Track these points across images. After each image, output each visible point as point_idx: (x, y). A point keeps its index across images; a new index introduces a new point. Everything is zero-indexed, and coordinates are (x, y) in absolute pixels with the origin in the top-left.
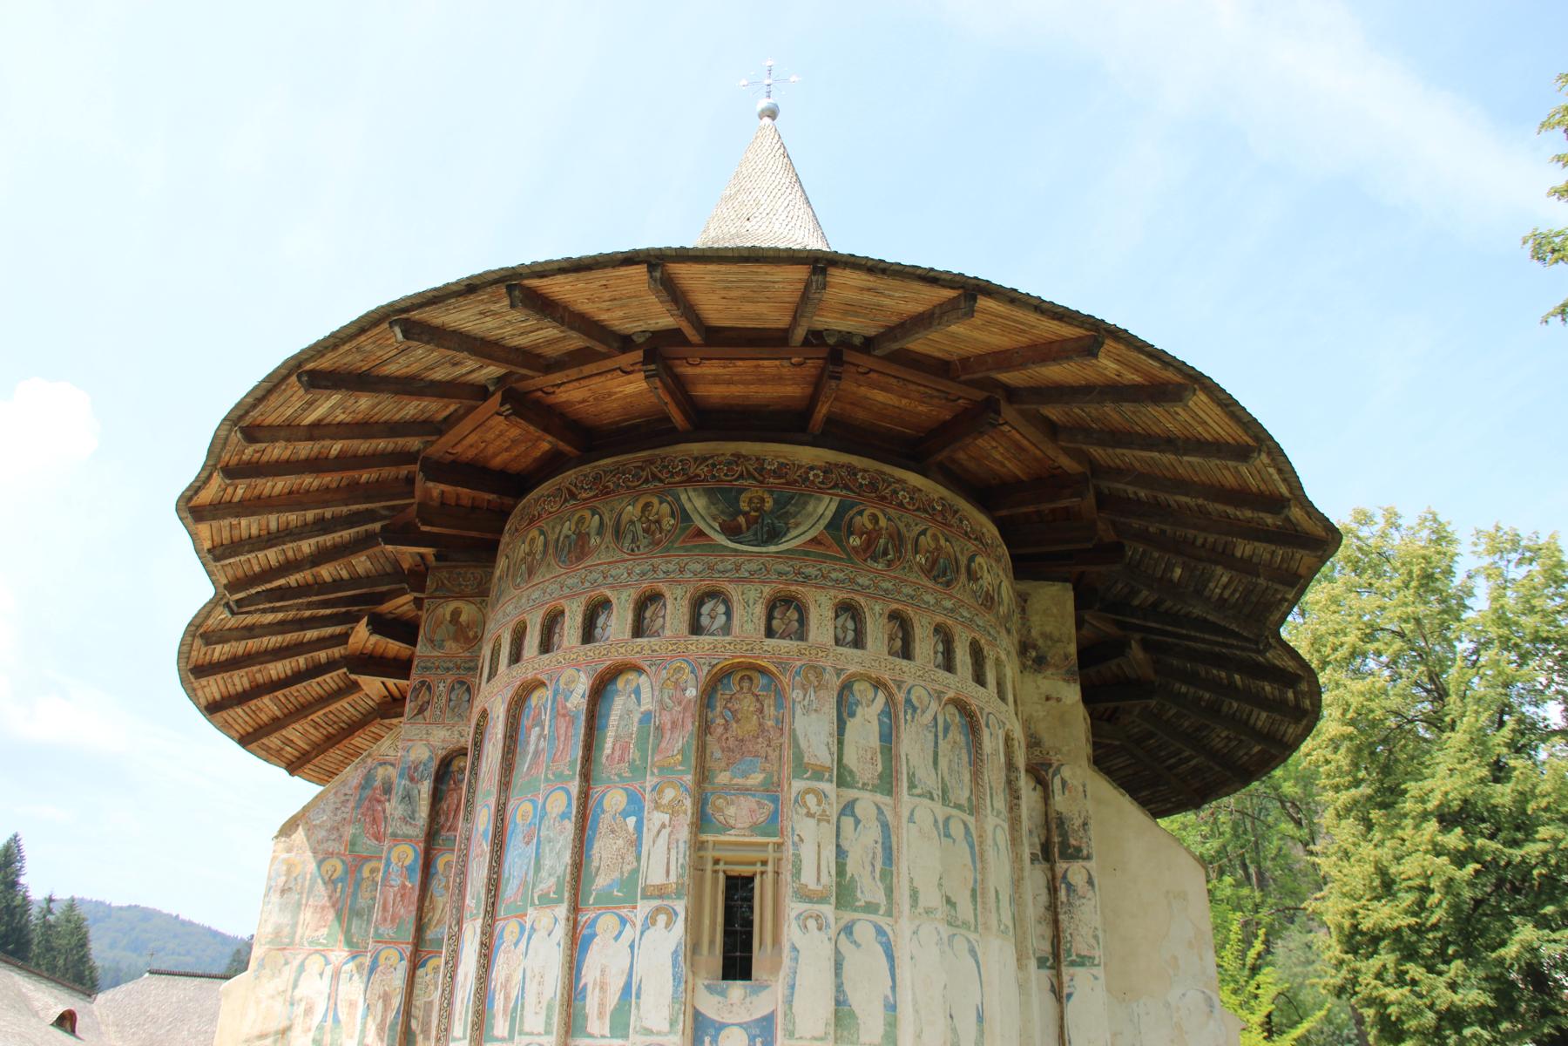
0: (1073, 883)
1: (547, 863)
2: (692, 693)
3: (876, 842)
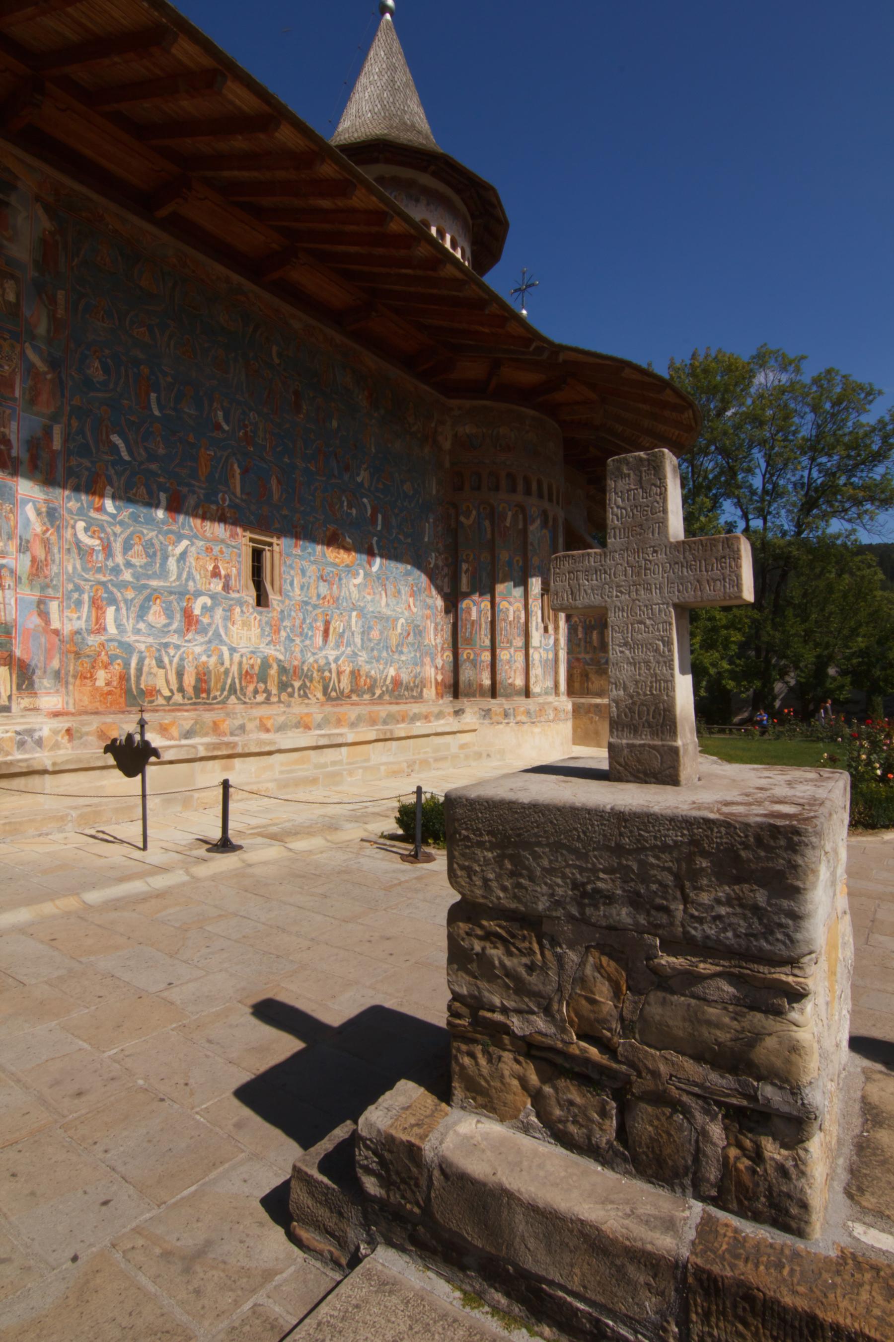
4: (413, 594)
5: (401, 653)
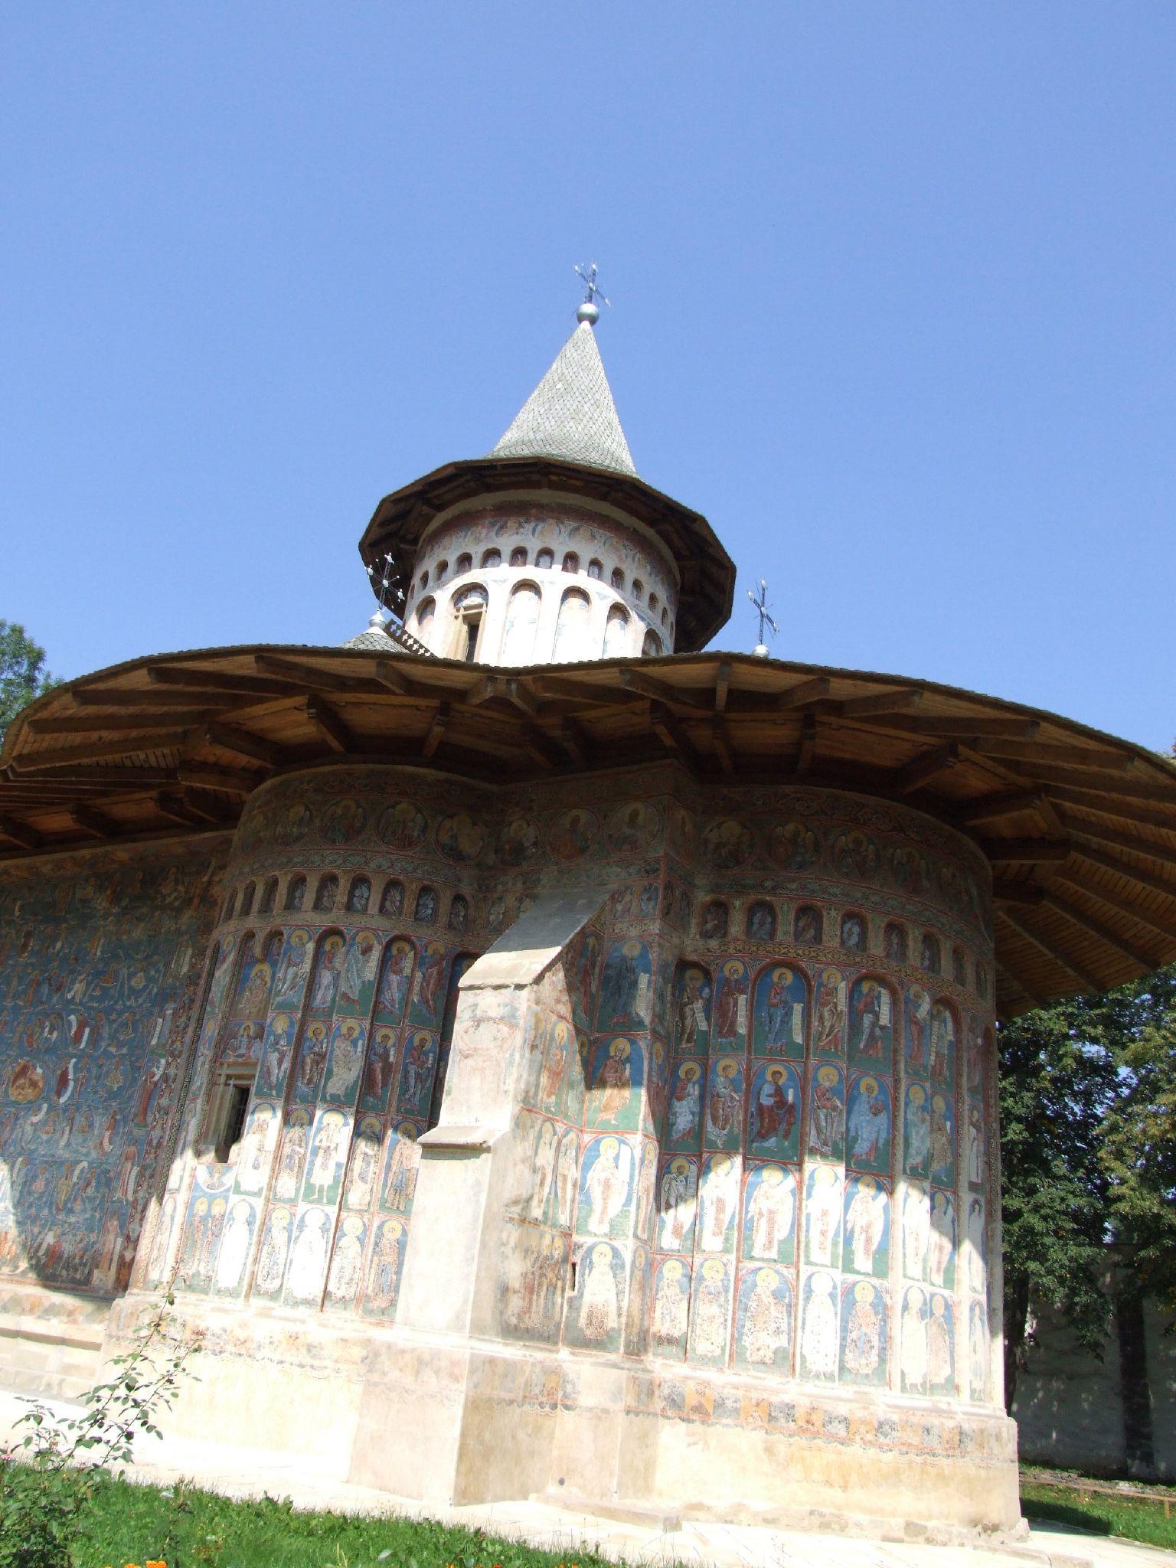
1: (915, 1142)
2: (979, 1041)
4: (114, 1126)
5: (71, 1211)
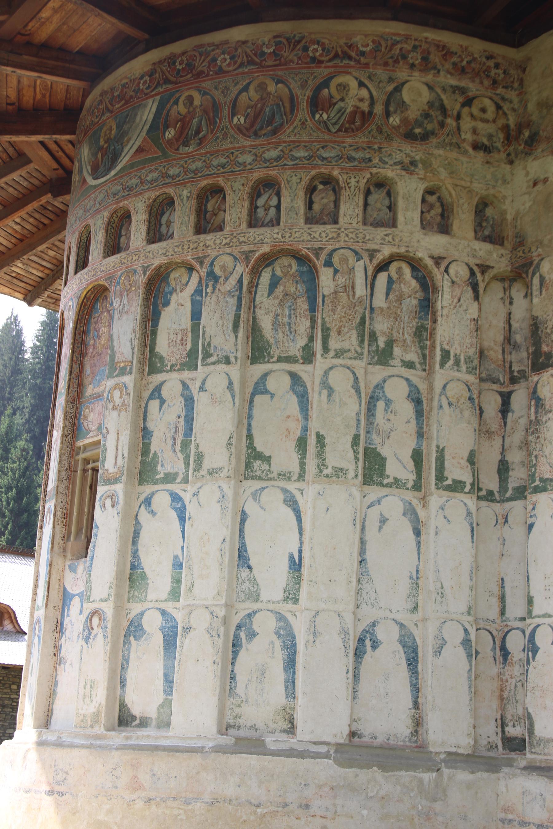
0: (542, 397)
3: (179, 417)
